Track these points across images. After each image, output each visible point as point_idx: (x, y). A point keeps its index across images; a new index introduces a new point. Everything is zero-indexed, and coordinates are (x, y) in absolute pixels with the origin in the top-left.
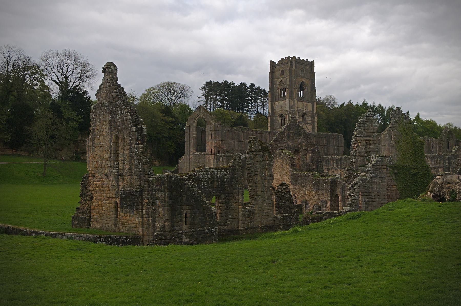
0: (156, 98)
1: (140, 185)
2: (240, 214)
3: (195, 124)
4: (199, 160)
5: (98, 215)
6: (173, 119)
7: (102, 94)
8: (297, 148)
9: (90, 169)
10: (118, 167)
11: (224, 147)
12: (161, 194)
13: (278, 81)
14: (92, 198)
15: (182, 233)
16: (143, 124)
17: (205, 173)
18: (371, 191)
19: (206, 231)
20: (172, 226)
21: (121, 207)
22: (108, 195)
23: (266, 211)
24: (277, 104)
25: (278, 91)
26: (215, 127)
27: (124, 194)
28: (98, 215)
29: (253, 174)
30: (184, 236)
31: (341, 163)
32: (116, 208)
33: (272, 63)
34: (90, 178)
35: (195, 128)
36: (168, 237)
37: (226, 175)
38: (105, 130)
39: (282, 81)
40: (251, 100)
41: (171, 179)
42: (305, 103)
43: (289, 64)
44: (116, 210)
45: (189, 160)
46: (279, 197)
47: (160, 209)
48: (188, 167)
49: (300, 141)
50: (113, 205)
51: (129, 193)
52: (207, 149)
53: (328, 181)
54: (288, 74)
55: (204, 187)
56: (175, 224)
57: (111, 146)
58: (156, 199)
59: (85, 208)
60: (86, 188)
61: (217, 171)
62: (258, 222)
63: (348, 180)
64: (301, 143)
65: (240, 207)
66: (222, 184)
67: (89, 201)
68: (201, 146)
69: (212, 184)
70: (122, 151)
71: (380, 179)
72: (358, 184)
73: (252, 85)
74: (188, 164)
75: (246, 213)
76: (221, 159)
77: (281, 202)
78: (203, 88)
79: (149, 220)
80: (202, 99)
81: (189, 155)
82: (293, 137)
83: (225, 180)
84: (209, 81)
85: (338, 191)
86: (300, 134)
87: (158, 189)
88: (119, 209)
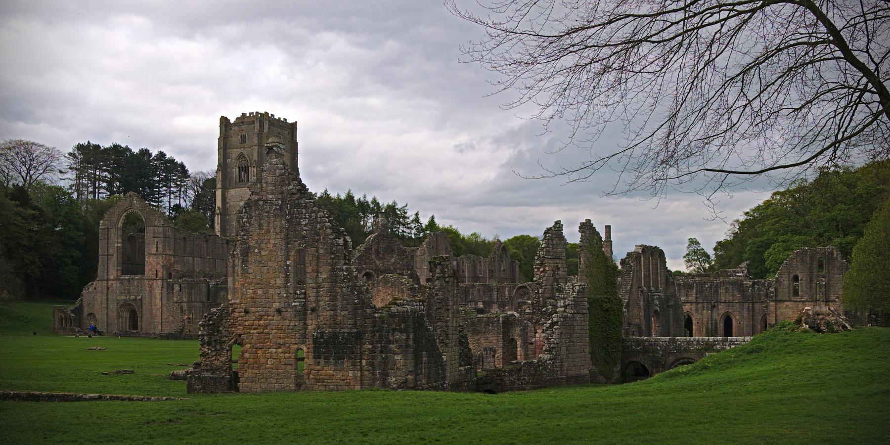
1: (355, 323)
3: (120, 225)
4: (129, 290)
5: (257, 371)
6: (37, 213)
7: (264, 185)
10: (305, 298)
11: (178, 267)
12: (398, 336)
13: (234, 153)
20: (416, 381)
24: (232, 192)
25: (236, 171)
26: (164, 233)
27: (322, 337)
28: (257, 371)
33: (224, 121)
35: (120, 233)
39: (242, 154)
43: (257, 125)
45: (108, 288)
48: (105, 301)
49: (393, 260)
51: (334, 336)
53: (499, 320)
57: (288, 266)
58: (389, 342)
68: (133, 264)
70: (315, 274)
73: (162, 155)
74: (105, 297)
76: (177, 287)
78: (70, 154)
79: (373, 374)
80: (68, 175)
81: (108, 280)
82: (384, 255)
84: (84, 142)
85: (516, 333)
86: (393, 251)
87: (394, 330)
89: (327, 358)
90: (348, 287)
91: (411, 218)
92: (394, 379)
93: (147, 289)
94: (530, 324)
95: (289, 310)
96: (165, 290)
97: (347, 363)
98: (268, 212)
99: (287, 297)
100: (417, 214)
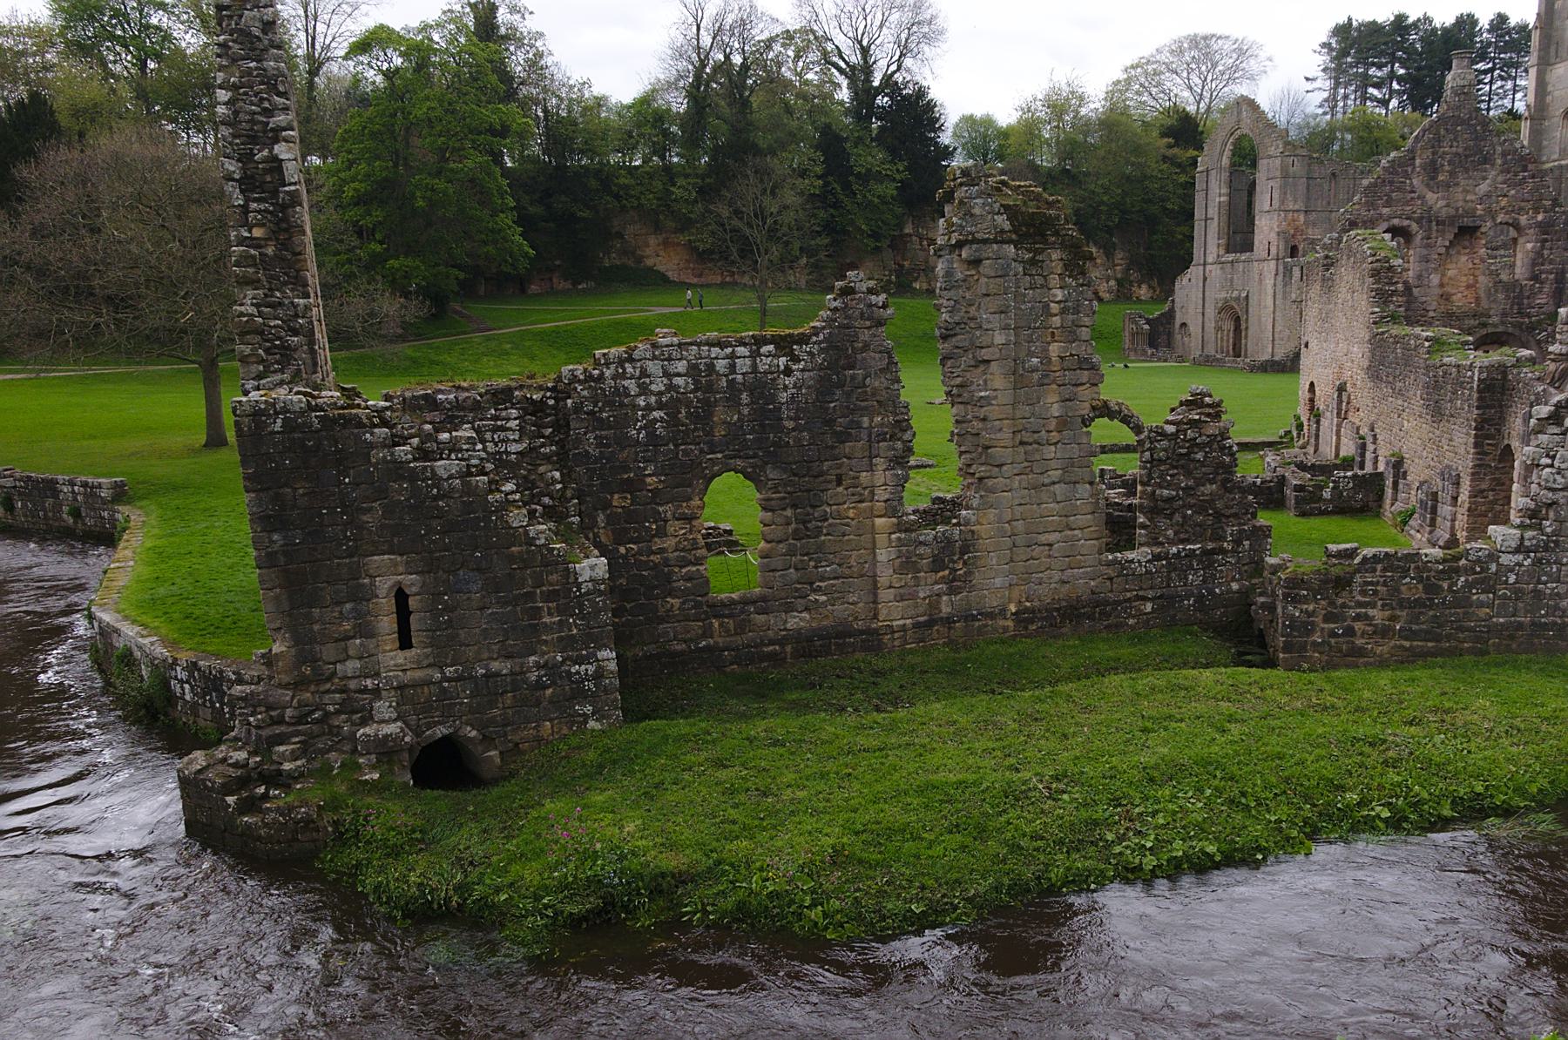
0: (1154, 91)
2: (883, 555)
3: (1225, 161)
8: (1467, 221)
17: (654, 367)
26: (1284, 169)
35: (1225, 175)
37: (788, 372)
40: (1492, 70)
41: (260, 426)
45: (1205, 279)
49: (1484, 188)
52: (1256, 242)
55: (651, 435)
61: (733, 356)
64: (1488, 195)
65: (879, 521)
68: (1240, 237)
75: (921, 550)
76: (1296, 272)
77: (1169, 486)
78: (1324, 45)
82: (1452, 174)
86: (1487, 160)
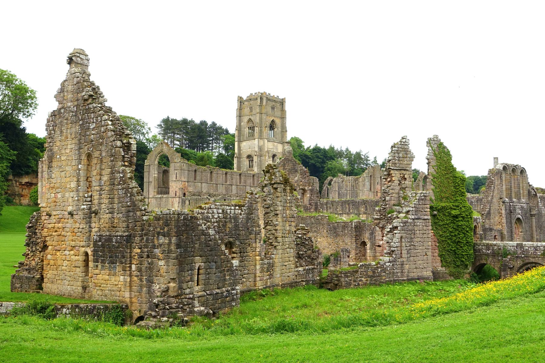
1: (128, 227)
2: (258, 267)
3: (156, 162)
4: (160, 204)
5: (55, 272)
7: (66, 94)
9: (44, 205)
10: (91, 201)
11: (191, 189)
12: (163, 240)
14: (45, 247)
15: (193, 299)
16: (130, 138)
17: (215, 211)
18: (413, 237)
19: (225, 294)
20: (180, 288)
21: (96, 261)
22: (73, 244)
23: (286, 263)
24: (244, 144)
26: (181, 167)
27: (100, 241)
28: (55, 272)
29: (272, 214)
30: (196, 303)
31: (327, 208)
32: (86, 261)
34: (43, 218)
35: (156, 167)
36: (174, 305)
37: (241, 214)
38: (69, 147)
39: (250, 119)
40: (212, 140)
41: (179, 217)
42: (276, 144)
43: (259, 100)
44: (87, 266)
46: (299, 244)
47: (161, 263)
49: (296, 178)
50: (81, 258)
51: (109, 239)
52: (170, 191)
53: (352, 224)
54: (258, 111)
56: (184, 286)
57: (79, 170)
58: (154, 247)
59: (33, 263)
60: (35, 233)
61: (231, 209)
62: (278, 279)
63: (379, 223)
64: (297, 181)
65: (257, 257)
66: (236, 226)
67: (40, 252)
69: (224, 226)
70: (98, 177)
71: (423, 221)
72: (399, 228)
73: (214, 124)
76: (187, 202)
77: (301, 251)
78: (158, 125)
79: (141, 280)
83: (240, 221)
85: (366, 237)
86: (296, 171)
87: (159, 234)
88: (91, 264)
89: (103, 262)
90: (123, 189)
91: (371, 161)
92: (158, 287)
93: (171, 203)
94: (378, 229)
95: (80, 213)
96: (180, 204)
97: (119, 268)
98: (67, 119)
99: (78, 200)
100: (375, 158)
